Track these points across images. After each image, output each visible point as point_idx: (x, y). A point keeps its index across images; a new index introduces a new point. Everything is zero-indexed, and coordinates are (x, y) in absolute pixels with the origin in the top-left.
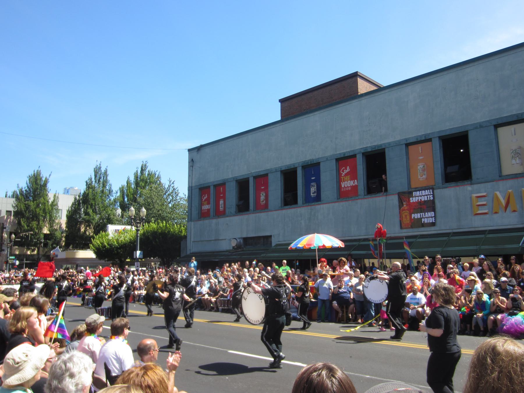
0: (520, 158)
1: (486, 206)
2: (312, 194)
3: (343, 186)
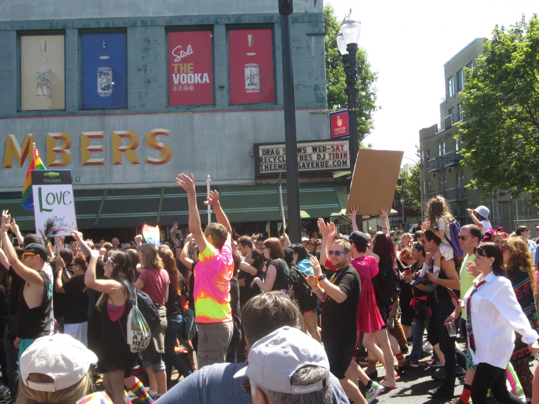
0: (48, 87)
2: (99, 91)
3: (176, 82)
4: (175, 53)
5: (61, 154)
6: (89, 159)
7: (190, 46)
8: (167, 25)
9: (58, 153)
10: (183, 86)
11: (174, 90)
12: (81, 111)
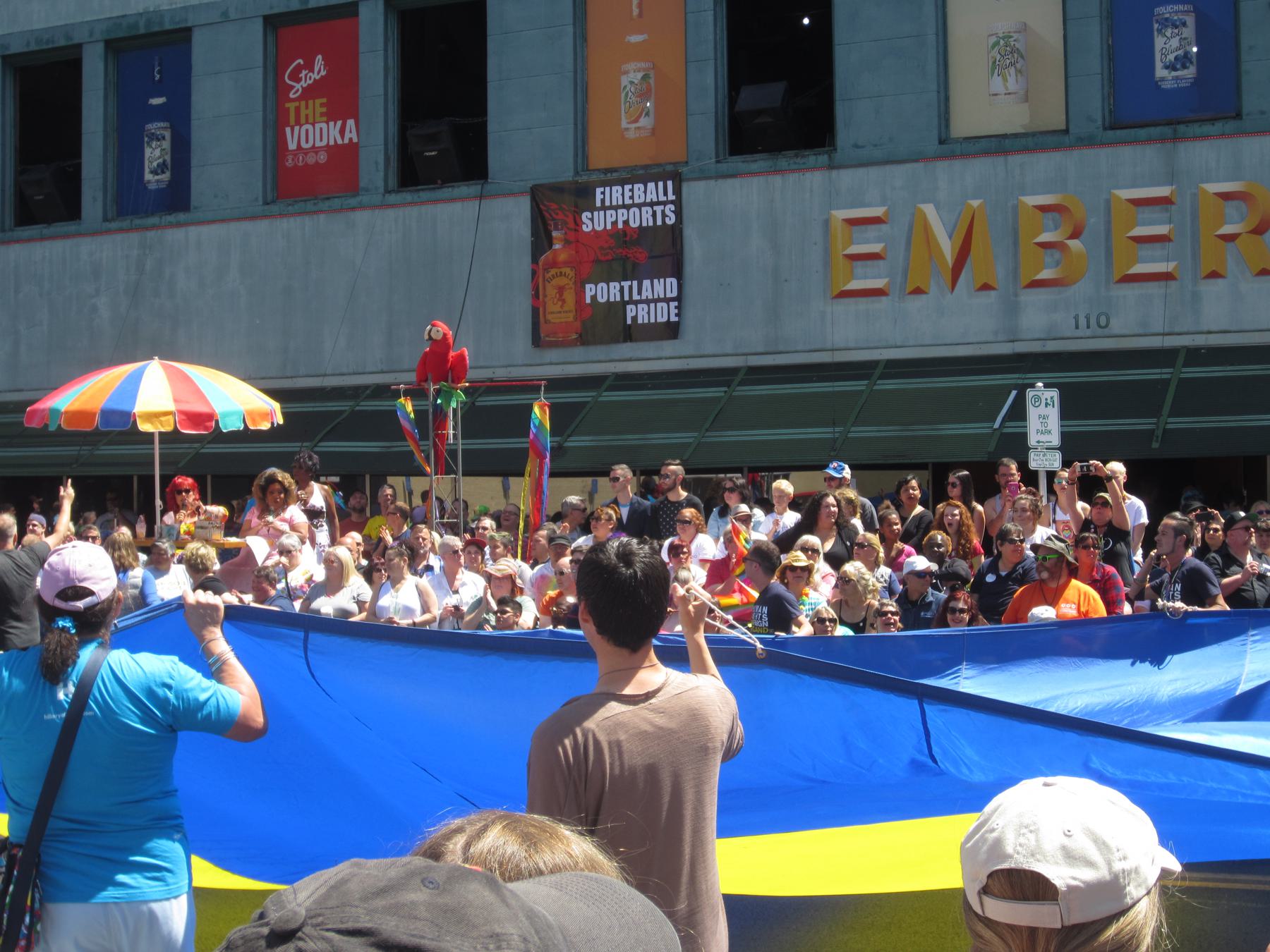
0: (1019, 71)
1: (881, 262)
2: (148, 176)
3: (292, 146)
4: (290, 78)
5: (1057, 254)
6: (849, 282)
7: (320, 57)
8: (113, 36)
9: (1049, 251)
10: (306, 154)
11: (287, 164)
12: (107, 223)
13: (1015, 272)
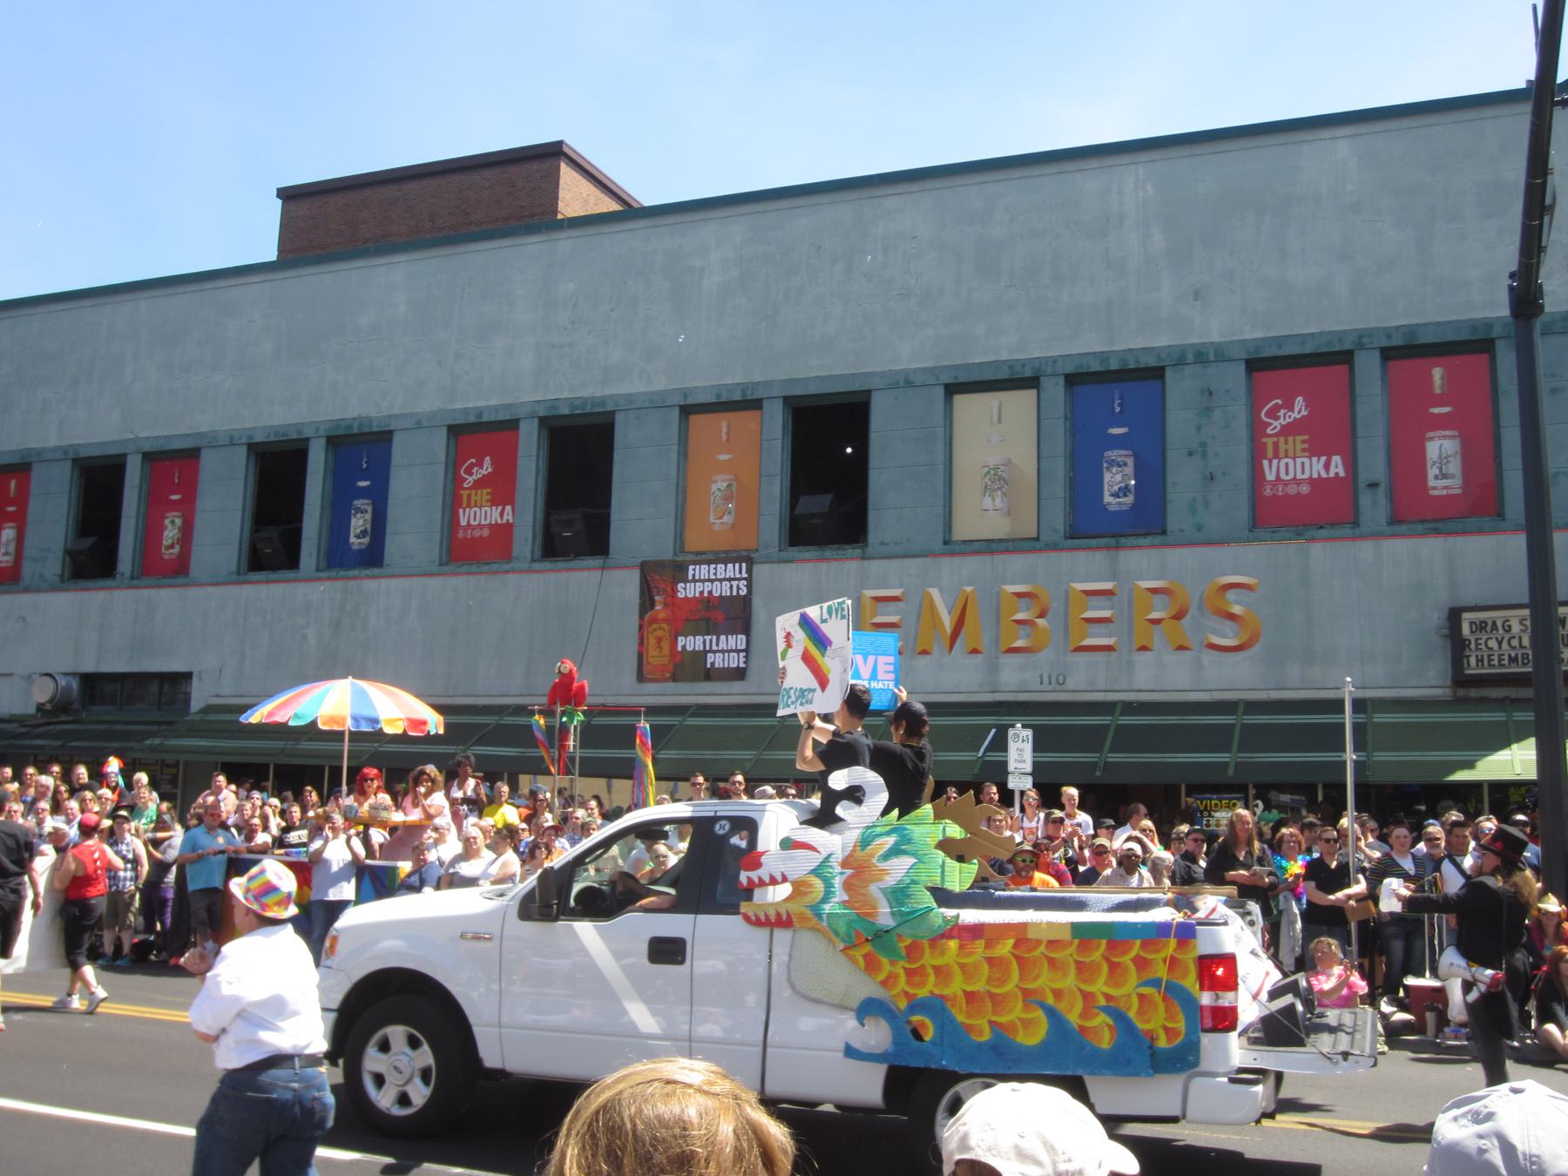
0: (1004, 494)
2: (1108, 499)
3: (1270, 477)
4: (1267, 415)
5: (1027, 628)
7: (1300, 399)
10: (1286, 485)
11: (1265, 493)
12: (1069, 541)
13: (997, 642)
